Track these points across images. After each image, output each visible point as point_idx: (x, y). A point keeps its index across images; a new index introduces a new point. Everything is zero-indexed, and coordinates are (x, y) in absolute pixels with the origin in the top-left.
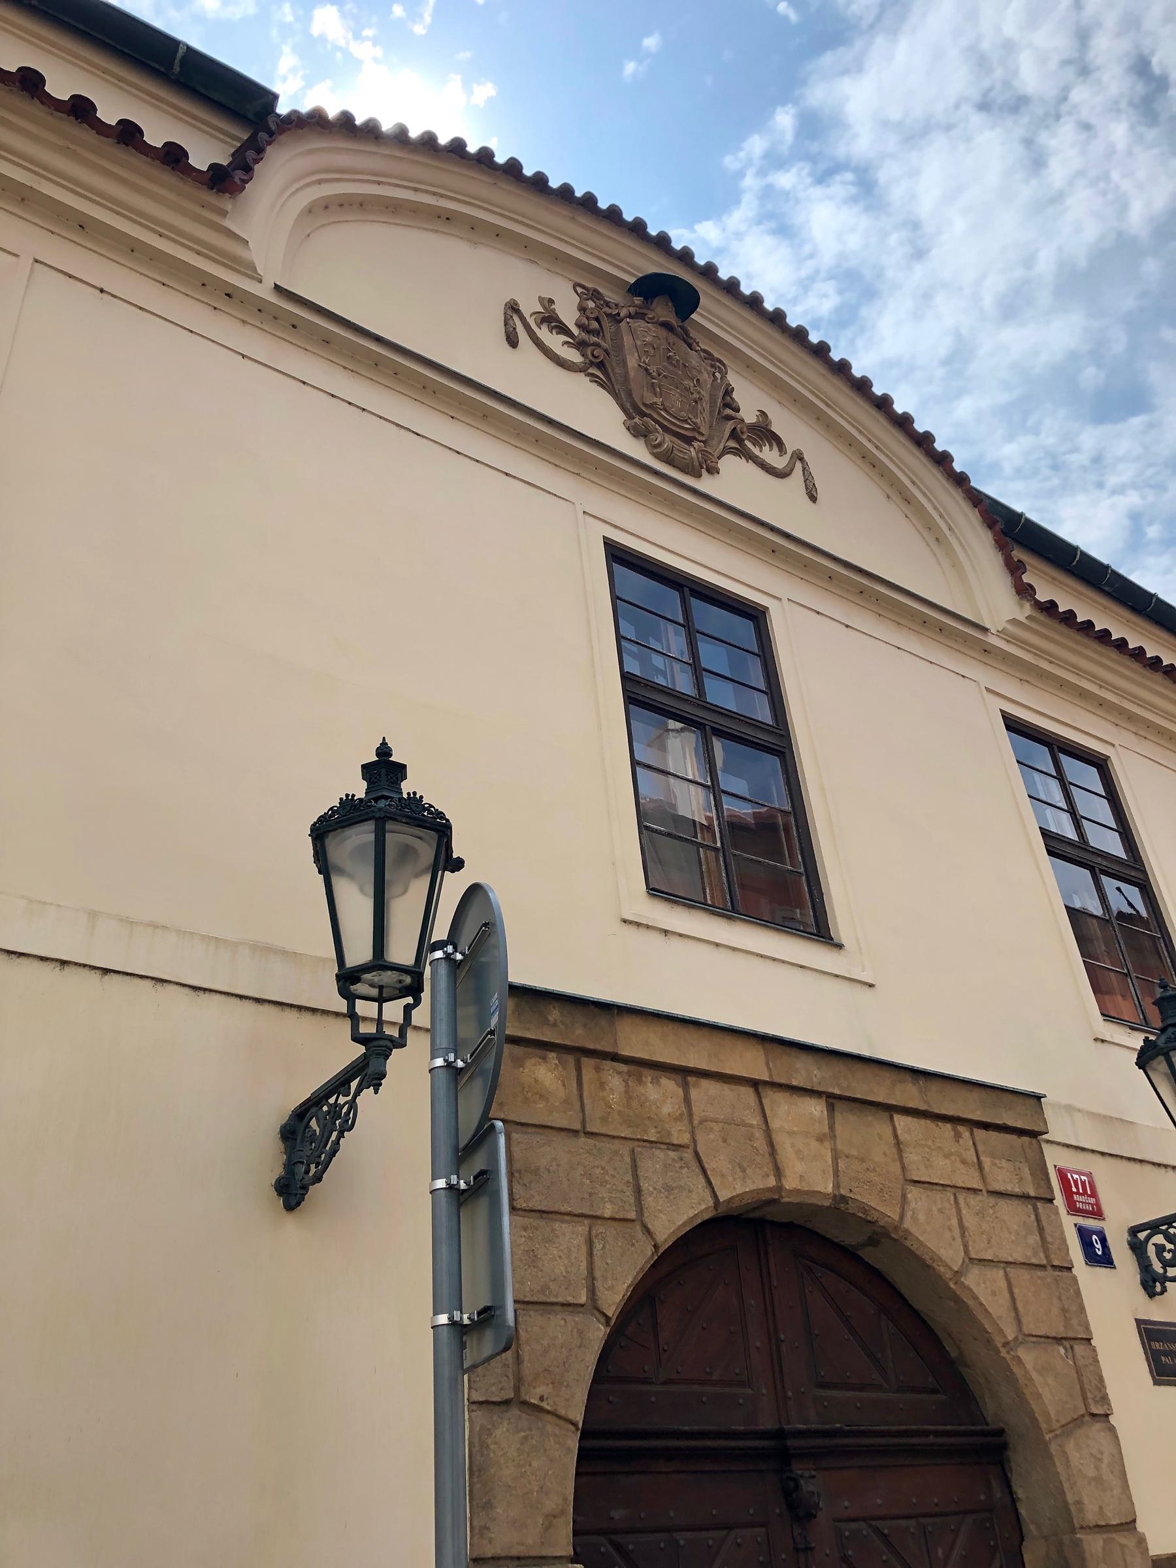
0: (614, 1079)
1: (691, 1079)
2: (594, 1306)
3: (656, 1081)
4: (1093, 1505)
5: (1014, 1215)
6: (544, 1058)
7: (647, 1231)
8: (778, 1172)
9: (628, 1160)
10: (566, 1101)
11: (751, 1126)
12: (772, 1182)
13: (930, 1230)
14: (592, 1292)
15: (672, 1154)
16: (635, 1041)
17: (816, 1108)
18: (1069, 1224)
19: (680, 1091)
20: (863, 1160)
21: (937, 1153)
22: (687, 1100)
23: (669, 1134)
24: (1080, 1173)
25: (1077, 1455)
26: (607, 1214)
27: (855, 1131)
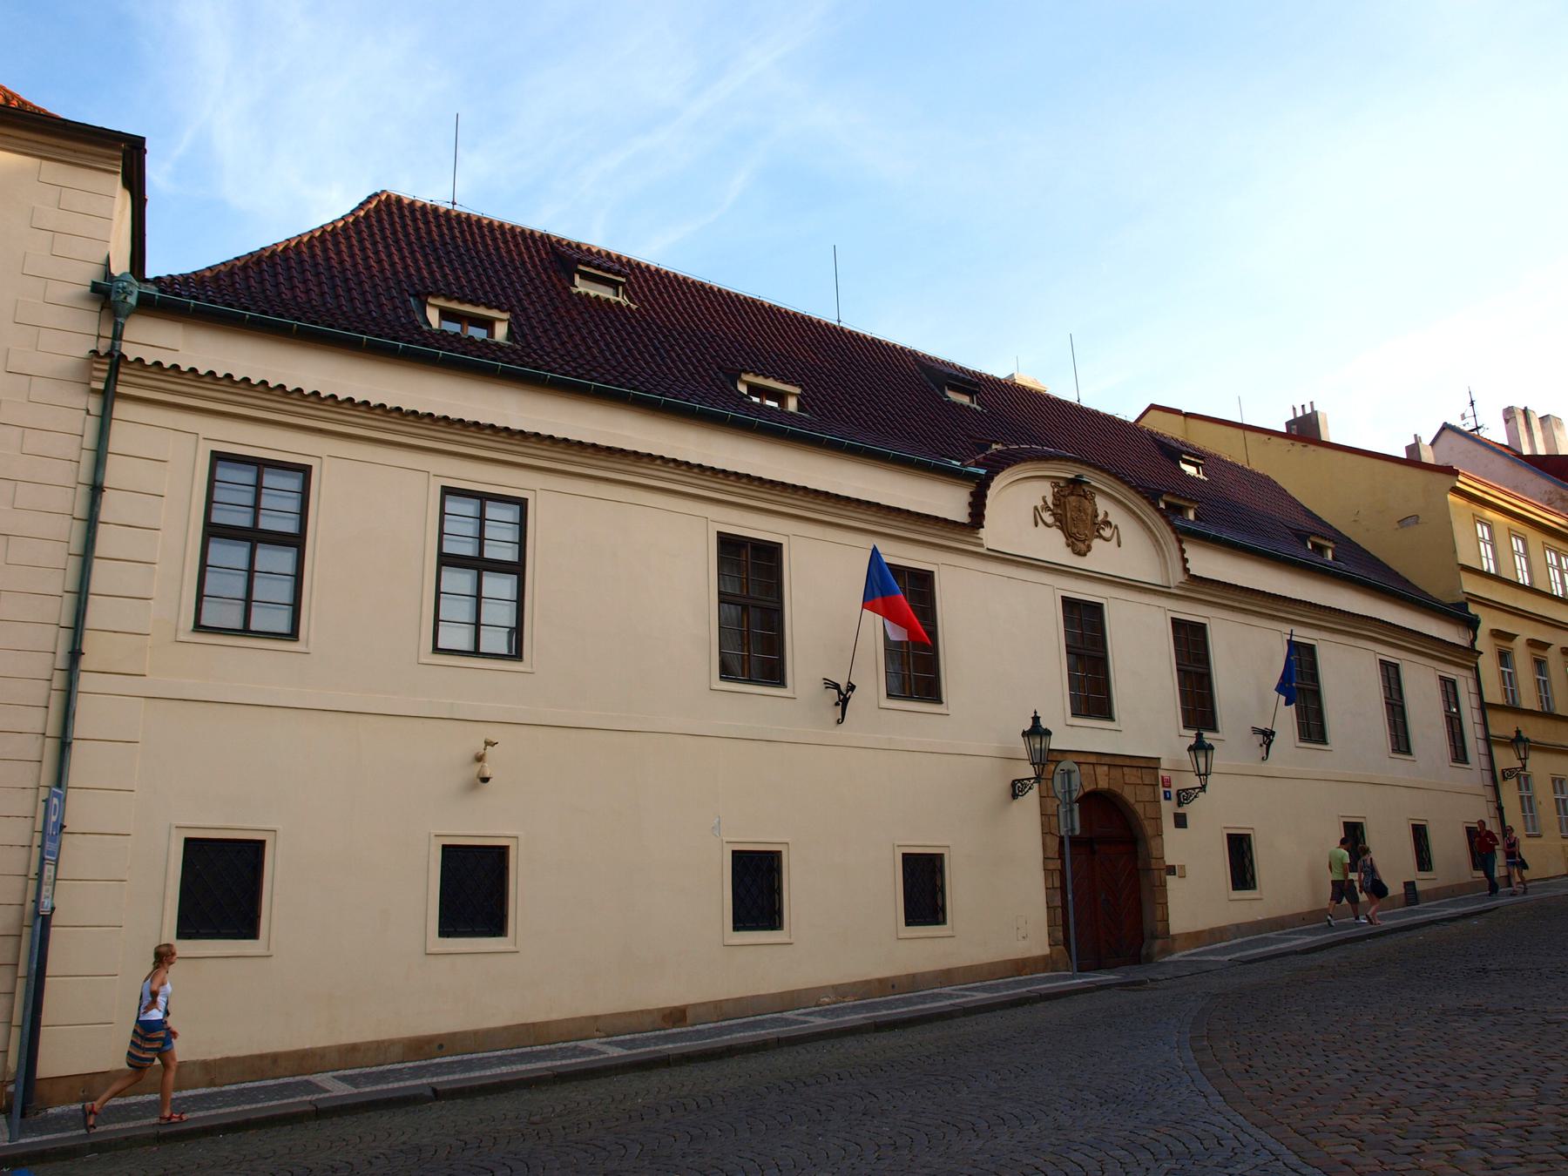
4: (1155, 854)
5: (1148, 790)
13: (1128, 794)
18: (1162, 790)
21: (1131, 776)
25: (1153, 844)
27: (1116, 773)
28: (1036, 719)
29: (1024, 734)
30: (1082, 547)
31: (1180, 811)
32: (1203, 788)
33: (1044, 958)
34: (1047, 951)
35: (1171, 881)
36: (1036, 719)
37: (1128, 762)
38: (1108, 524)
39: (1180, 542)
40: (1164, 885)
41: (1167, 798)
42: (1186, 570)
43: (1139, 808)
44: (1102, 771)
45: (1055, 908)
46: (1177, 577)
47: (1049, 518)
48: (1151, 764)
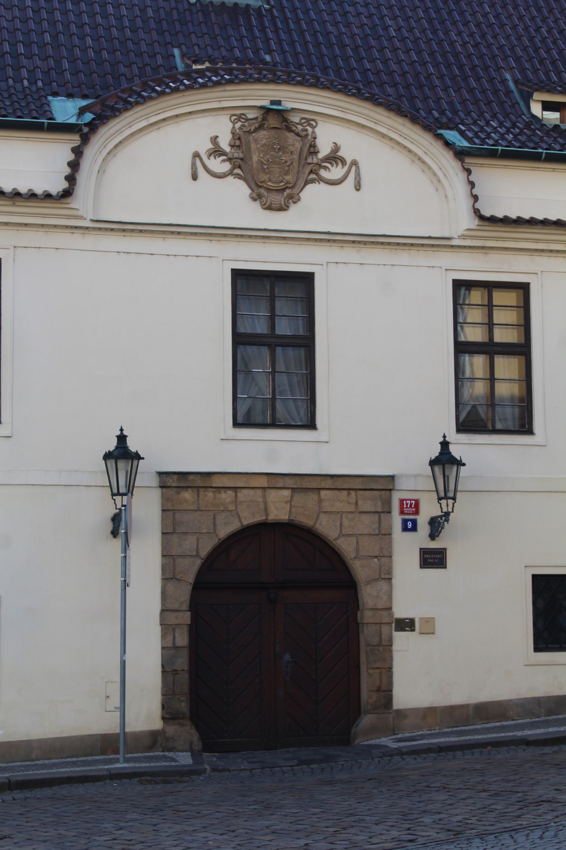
0: (210, 494)
1: (238, 490)
2: (198, 555)
3: (225, 492)
6: (187, 491)
7: (217, 535)
8: (267, 514)
9: (212, 517)
10: (194, 503)
11: (259, 502)
12: (264, 518)
13: (327, 528)
14: (197, 552)
15: (228, 513)
16: (217, 482)
17: (287, 493)
19: (234, 494)
20: (303, 507)
22: (236, 496)
23: (228, 507)
24: (411, 500)
26: (204, 532)
28: (122, 438)
29: (107, 456)
30: (278, 199)
31: (433, 545)
32: (447, 514)
33: (154, 734)
34: (157, 724)
35: (400, 639)
36: (122, 438)
37: (329, 483)
38: (334, 158)
39: (469, 172)
40: (387, 646)
41: (410, 526)
42: (477, 212)
43: (347, 547)
44: (273, 495)
45: (175, 672)
46: (465, 221)
47: (224, 167)
48: (383, 485)
